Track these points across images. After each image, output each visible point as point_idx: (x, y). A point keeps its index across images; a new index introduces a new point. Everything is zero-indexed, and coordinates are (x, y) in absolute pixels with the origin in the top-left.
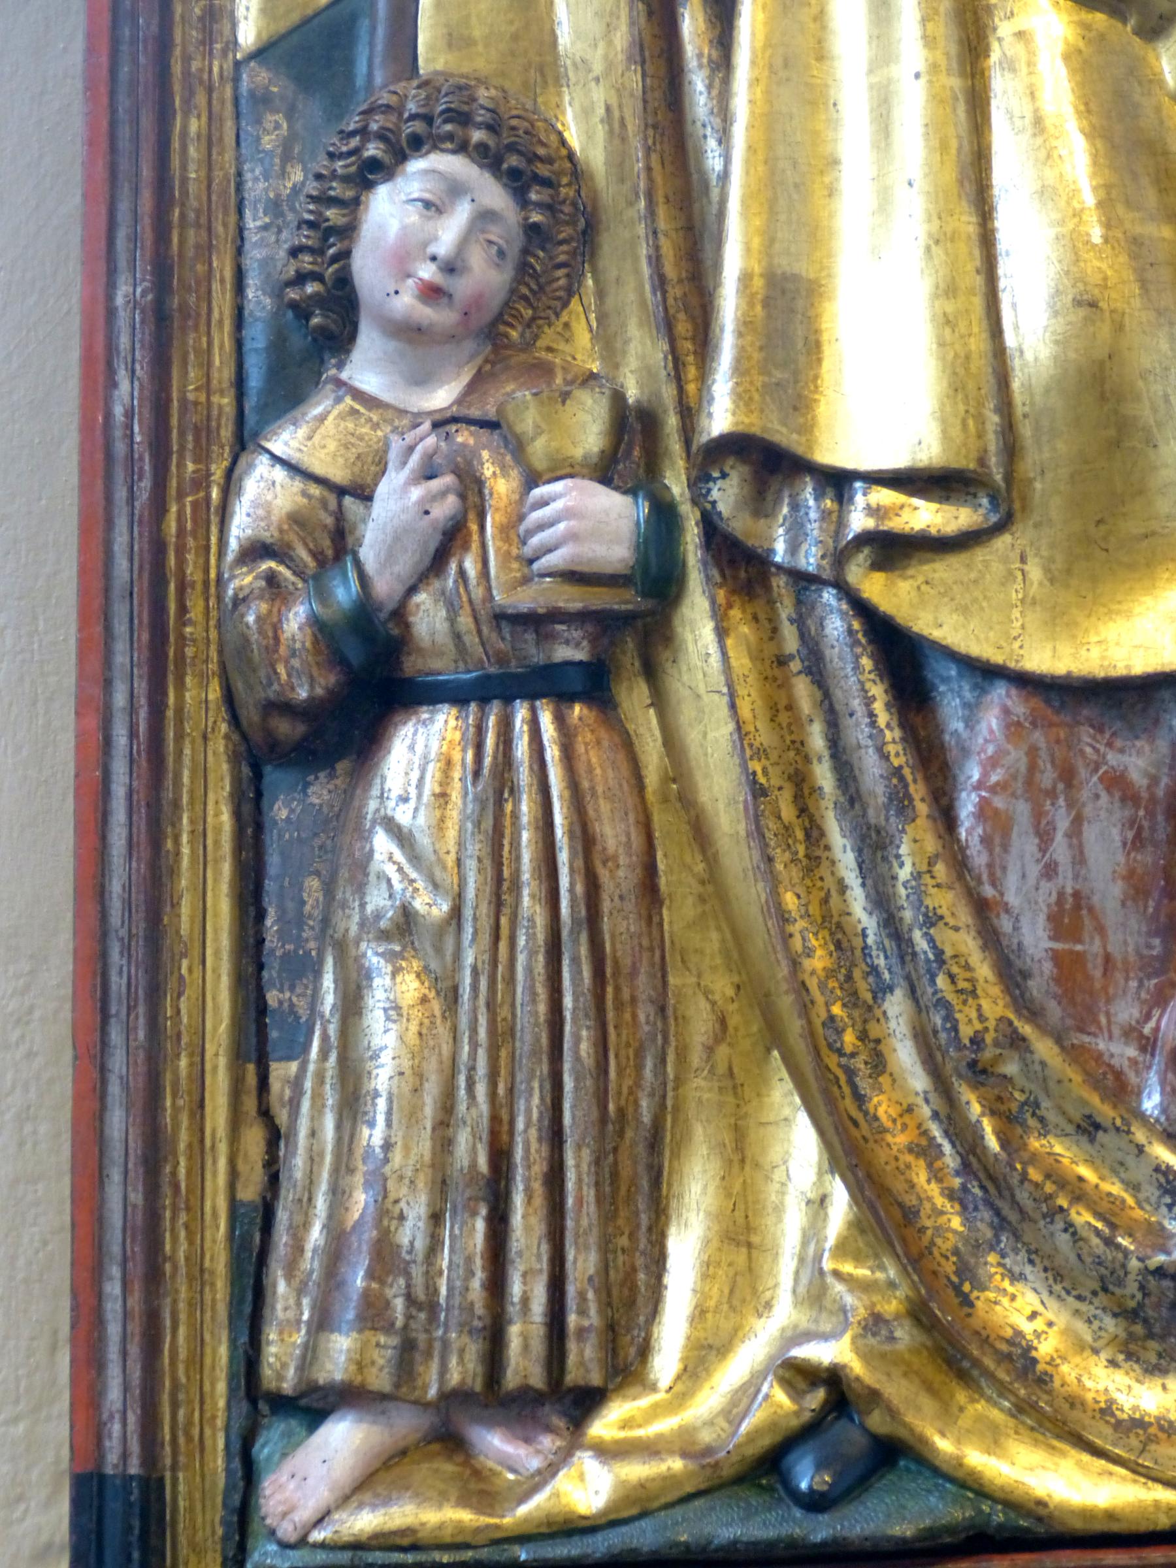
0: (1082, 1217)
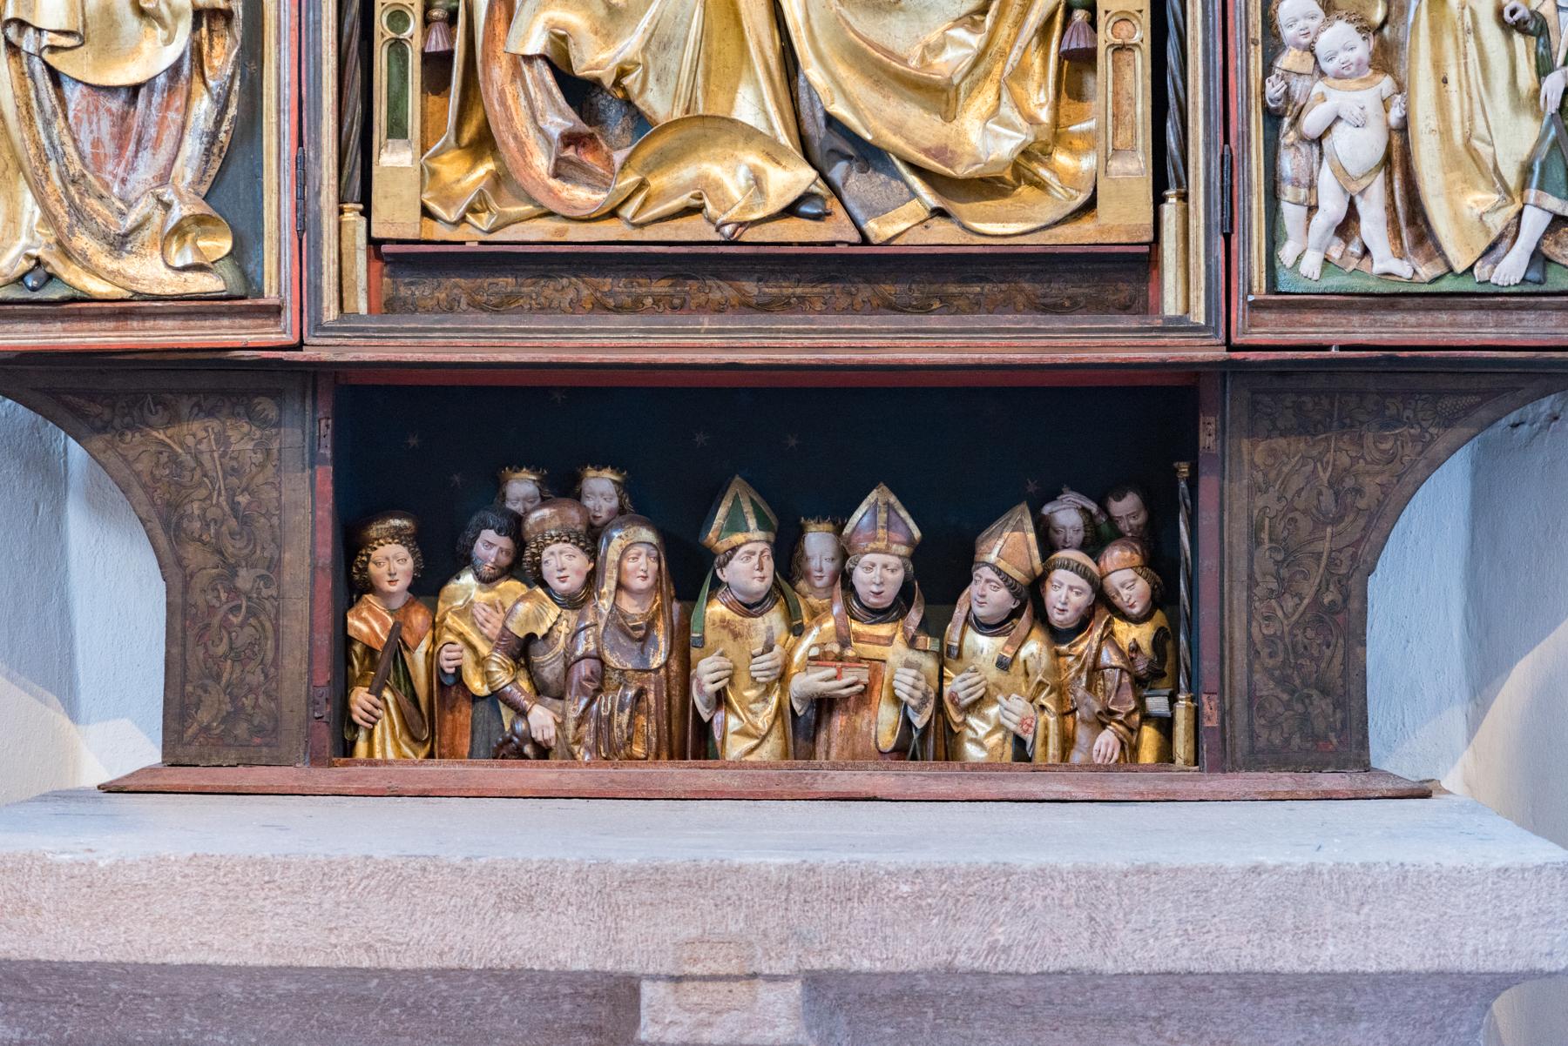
0: (99, 220)
